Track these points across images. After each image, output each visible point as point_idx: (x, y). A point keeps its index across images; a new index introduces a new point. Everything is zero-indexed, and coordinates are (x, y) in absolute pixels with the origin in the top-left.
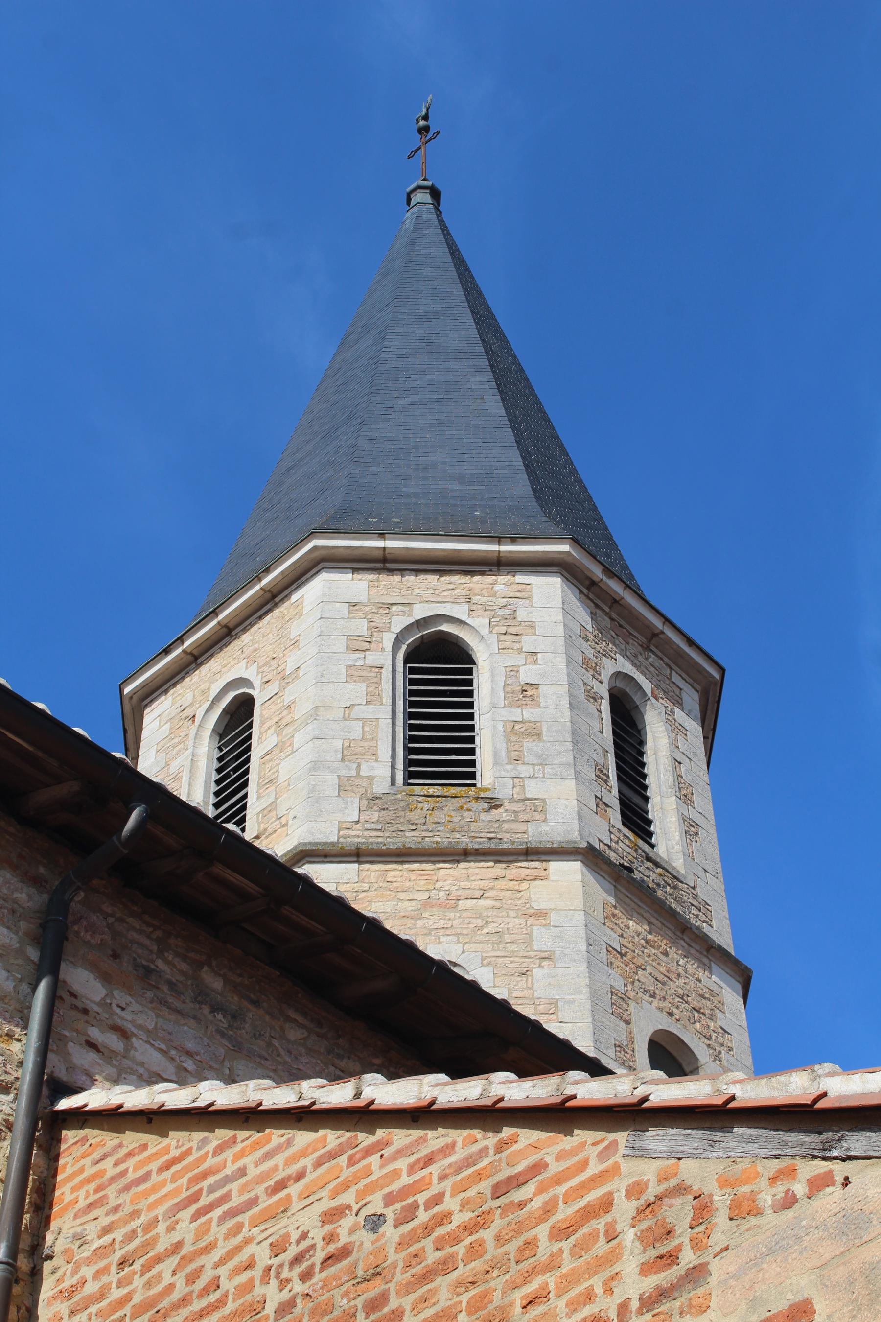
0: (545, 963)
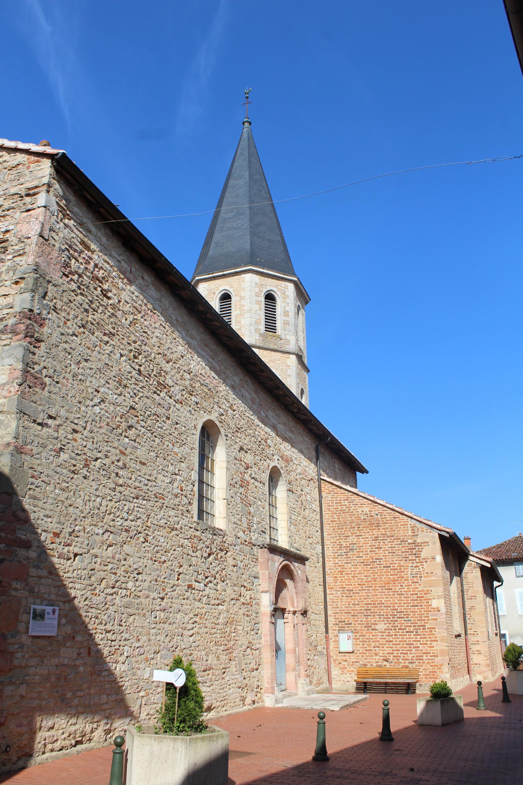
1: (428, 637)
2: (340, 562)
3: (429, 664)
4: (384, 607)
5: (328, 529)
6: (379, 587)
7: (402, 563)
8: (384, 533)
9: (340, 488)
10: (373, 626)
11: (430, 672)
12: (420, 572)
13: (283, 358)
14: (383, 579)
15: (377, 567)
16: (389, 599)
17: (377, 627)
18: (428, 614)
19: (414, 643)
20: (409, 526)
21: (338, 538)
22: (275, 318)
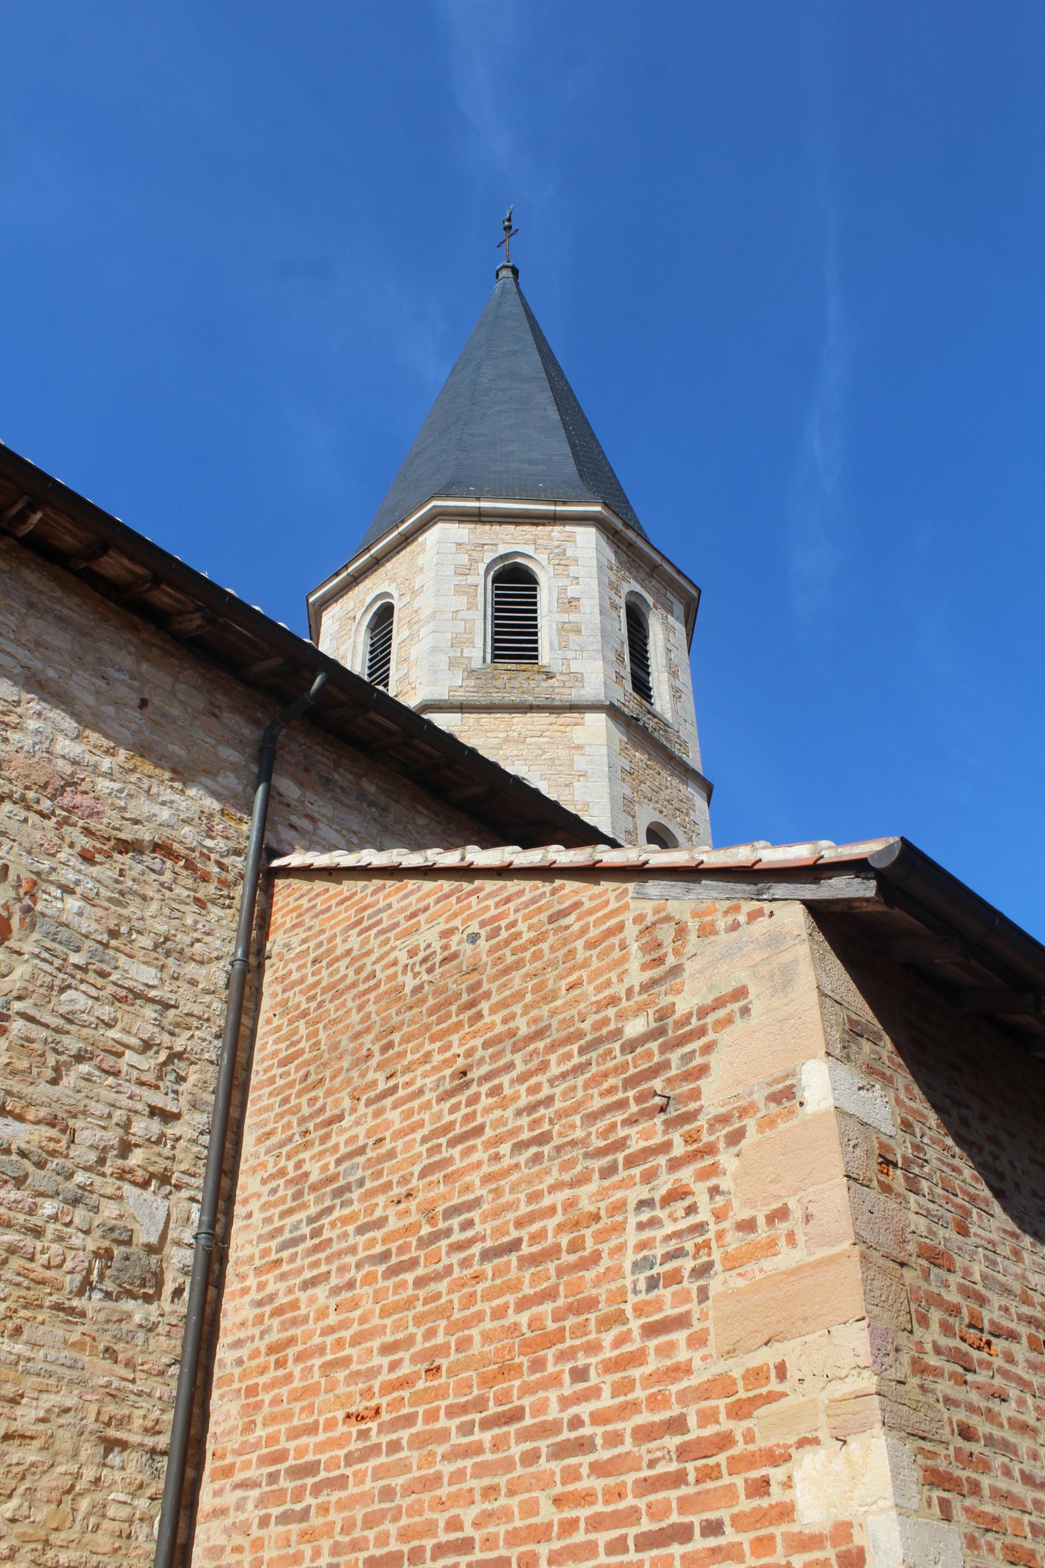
0: (581, 779)
7: (586, 1196)
12: (699, 1228)
13: (555, 727)
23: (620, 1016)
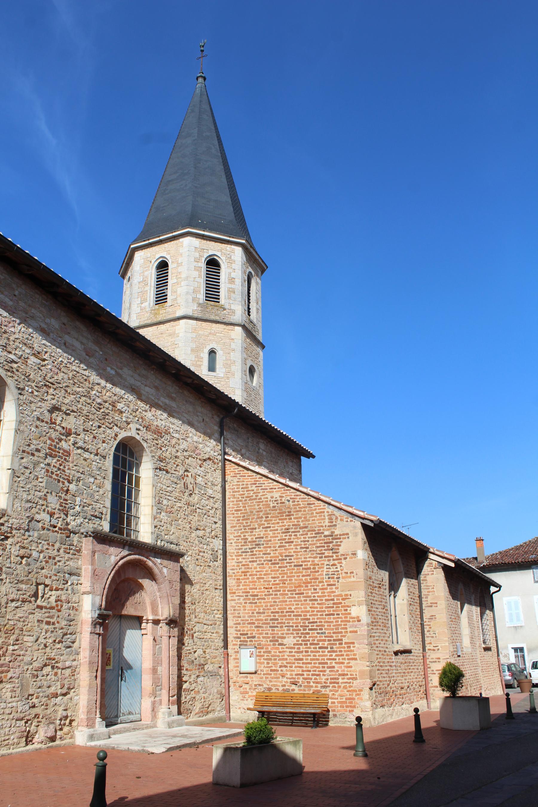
1: (345, 654)
2: (244, 561)
3: (346, 688)
4: (294, 616)
5: (232, 520)
6: (288, 591)
7: (316, 561)
8: (296, 523)
9: (248, 469)
10: (280, 640)
11: (346, 699)
12: (338, 571)
13: (225, 330)
14: (293, 581)
15: (286, 567)
16: (300, 606)
17: (285, 641)
18: (346, 625)
19: (329, 662)
20: (326, 514)
21: (243, 530)
22: (219, 286)
23: (323, 530)
